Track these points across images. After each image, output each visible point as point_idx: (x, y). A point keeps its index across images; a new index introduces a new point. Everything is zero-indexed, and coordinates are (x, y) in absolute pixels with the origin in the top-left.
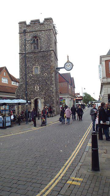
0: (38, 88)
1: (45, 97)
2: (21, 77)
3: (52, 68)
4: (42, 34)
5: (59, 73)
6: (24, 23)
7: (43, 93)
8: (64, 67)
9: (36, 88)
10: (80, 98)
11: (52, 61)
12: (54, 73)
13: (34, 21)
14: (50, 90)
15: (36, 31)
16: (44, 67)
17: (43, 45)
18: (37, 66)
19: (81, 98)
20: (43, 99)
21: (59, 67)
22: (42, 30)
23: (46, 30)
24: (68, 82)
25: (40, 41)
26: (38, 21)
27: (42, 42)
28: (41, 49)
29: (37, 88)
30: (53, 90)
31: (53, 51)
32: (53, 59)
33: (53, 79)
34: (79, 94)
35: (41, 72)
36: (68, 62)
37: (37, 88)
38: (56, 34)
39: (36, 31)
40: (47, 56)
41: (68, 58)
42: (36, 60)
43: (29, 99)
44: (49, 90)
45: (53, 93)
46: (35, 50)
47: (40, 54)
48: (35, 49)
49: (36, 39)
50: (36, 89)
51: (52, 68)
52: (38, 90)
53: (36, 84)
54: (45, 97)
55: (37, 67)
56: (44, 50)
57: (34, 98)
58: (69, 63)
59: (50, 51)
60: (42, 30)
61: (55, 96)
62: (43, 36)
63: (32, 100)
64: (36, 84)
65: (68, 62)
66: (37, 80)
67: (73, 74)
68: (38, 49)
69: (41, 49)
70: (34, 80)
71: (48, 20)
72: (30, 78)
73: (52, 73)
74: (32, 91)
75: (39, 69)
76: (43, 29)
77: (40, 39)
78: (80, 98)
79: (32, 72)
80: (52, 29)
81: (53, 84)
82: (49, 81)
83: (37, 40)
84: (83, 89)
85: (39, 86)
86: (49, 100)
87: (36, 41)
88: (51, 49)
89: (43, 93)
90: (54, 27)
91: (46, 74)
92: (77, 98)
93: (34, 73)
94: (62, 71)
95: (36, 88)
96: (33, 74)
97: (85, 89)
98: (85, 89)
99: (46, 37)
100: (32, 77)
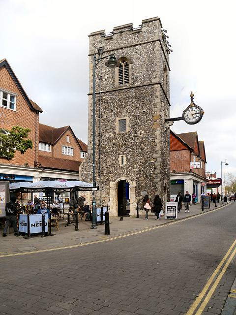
0: (124, 160)
1: (138, 178)
3: (155, 118)
5: (172, 133)
6: (100, 34)
7: (135, 169)
8: (181, 116)
9: (120, 159)
10: (215, 182)
11: (155, 105)
12: (159, 129)
13: (121, 29)
14: (150, 164)
15: (125, 48)
16: (139, 117)
17: (138, 74)
18: (124, 116)
19: (218, 181)
20: (134, 182)
21: (171, 117)
24: (191, 150)
25: (132, 67)
26: (129, 27)
28: (133, 83)
29: (123, 160)
31: (160, 84)
32: (157, 101)
33: (156, 140)
34: (214, 176)
35: (133, 127)
36: (193, 105)
37: (123, 160)
38: (168, 51)
39: (125, 48)
40: (146, 96)
41: (192, 99)
43: (106, 181)
44: (147, 164)
46: (121, 85)
47: (131, 93)
48: (121, 83)
49: (123, 64)
50: (120, 163)
51: (155, 118)
52: (125, 163)
53: (121, 153)
54: (138, 178)
55: (124, 118)
56: (140, 83)
57: (117, 178)
58: (194, 109)
59: (154, 84)
61: (159, 175)
62: (138, 56)
63: (113, 185)
64: (121, 153)
65: (193, 105)
66: (122, 145)
67: (203, 132)
68: (127, 82)
69: (133, 83)
70: (117, 145)
71: (149, 22)
73: (156, 130)
75: (128, 123)
77: (131, 63)
78: (215, 182)
79: (113, 128)
80: (159, 40)
81: (156, 152)
82: (148, 145)
83: (127, 65)
84: (224, 165)
85: (126, 156)
87: (124, 67)
88: (154, 81)
89: (135, 169)
90: (164, 37)
91: (143, 132)
92: (210, 182)
93: (117, 131)
94: (179, 128)
95: (120, 159)
96: (114, 133)
97: (227, 164)
98: (227, 164)
99: (145, 58)
100: (114, 138)
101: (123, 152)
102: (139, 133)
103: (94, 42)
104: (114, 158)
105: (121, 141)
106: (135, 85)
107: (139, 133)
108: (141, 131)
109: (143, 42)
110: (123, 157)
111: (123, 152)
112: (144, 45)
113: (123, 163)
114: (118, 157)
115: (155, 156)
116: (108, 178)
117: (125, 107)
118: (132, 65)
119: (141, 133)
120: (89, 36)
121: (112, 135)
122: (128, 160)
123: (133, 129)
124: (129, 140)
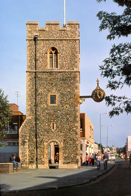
0: (55, 127)
1: (64, 141)
2: (29, 108)
4: (63, 46)
20: (62, 143)
22: (64, 40)
23: (69, 40)
27: (63, 57)
30: (77, 130)
37: (53, 126)
42: (52, 84)
43: (41, 142)
45: (76, 134)
53: (52, 121)
55: (54, 94)
57: (49, 140)
60: (64, 40)
64: (52, 121)
70: (50, 114)
72: (44, 110)
74: (45, 130)
76: (65, 39)
85: (56, 123)
86: (70, 144)
89: (62, 134)
100: (46, 109)
101: (54, 120)
102: (65, 106)
103: (30, 30)
104: (47, 124)
105: (52, 111)
106: (62, 70)
107: (65, 106)
108: (66, 105)
109: (68, 38)
110: (53, 124)
111: (54, 120)
112: (68, 41)
113: (53, 129)
114: (50, 124)
115: (76, 124)
116: (42, 140)
117: (55, 85)
118: (60, 54)
119: (66, 107)
120: (27, 24)
121: (45, 106)
122: (57, 127)
123: (61, 103)
124: (58, 112)
